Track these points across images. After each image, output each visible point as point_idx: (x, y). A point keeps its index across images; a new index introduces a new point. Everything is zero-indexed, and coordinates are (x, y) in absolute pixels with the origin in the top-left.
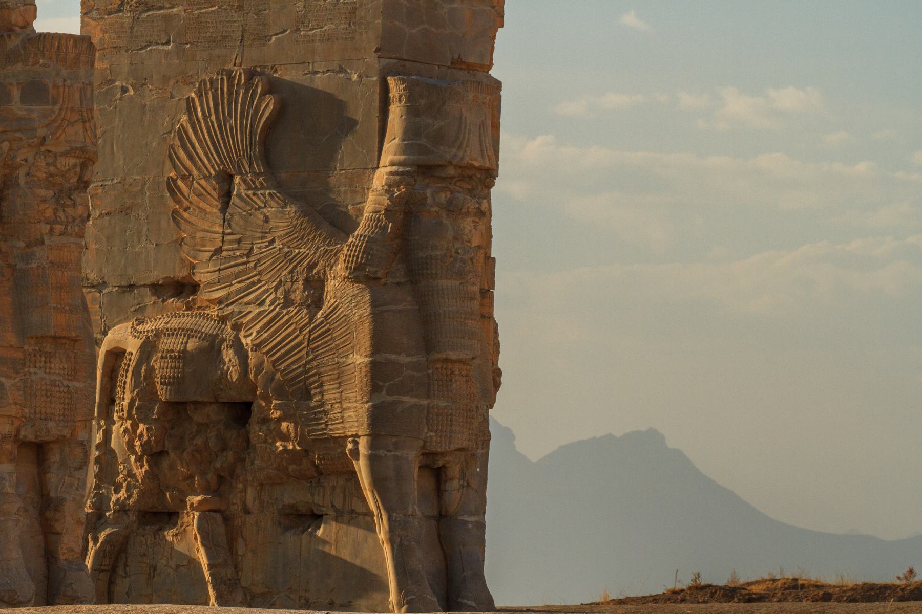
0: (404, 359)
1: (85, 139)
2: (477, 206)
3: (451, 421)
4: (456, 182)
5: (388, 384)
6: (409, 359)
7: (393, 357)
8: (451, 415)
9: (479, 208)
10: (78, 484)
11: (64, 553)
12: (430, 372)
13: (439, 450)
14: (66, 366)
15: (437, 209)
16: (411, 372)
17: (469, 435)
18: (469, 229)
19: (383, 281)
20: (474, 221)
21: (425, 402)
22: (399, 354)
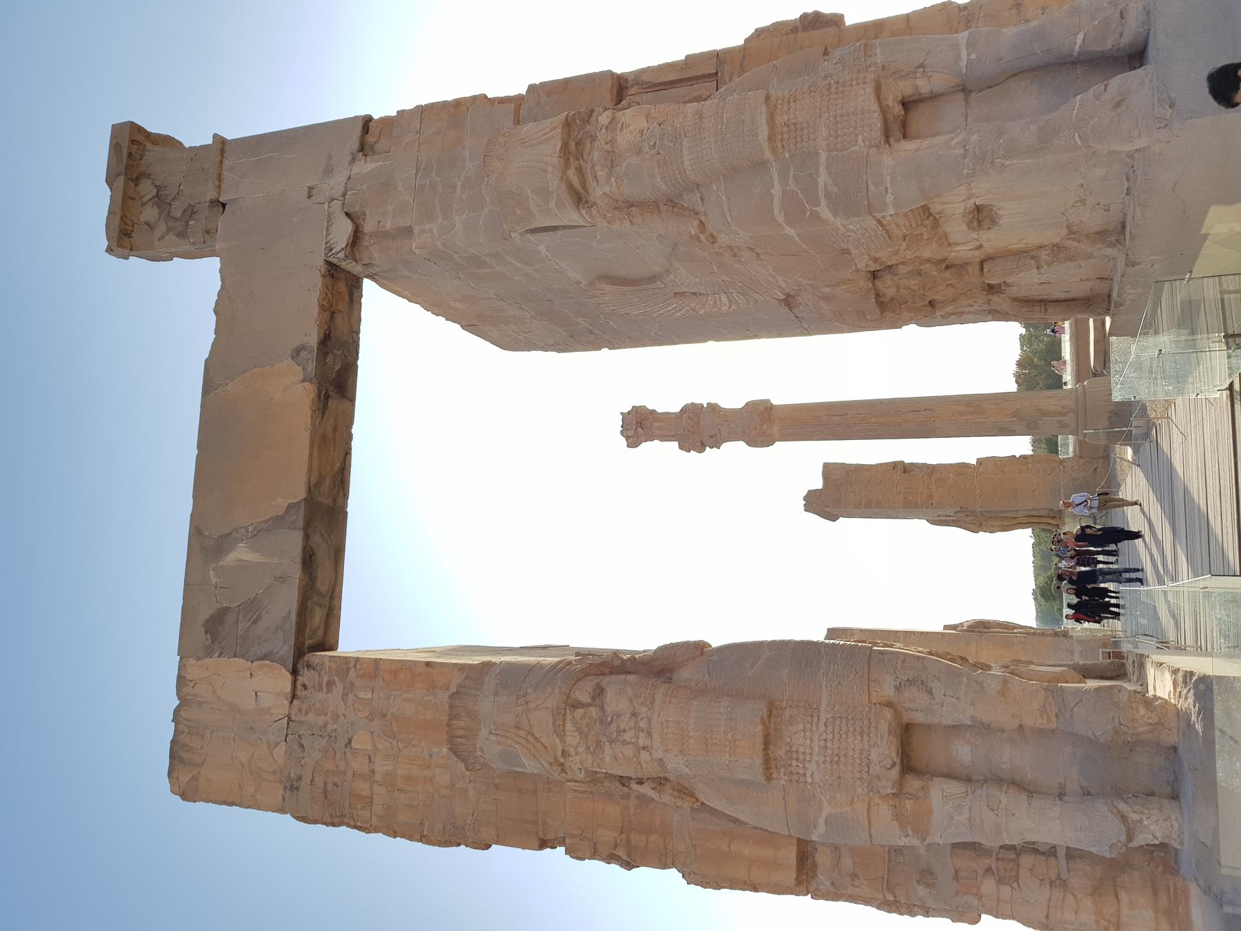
0: (777, 191)
1: (546, 708)
2: (604, 130)
3: (842, 116)
4: (584, 161)
5: (807, 206)
6: (776, 183)
8: (835, 117)
9: (607, 128)
11: (1049, 719)
12: (787, 155)
13: (879, 125)
14: (801, 727)
15: (613, 180)
16: (791, 180)
17: (858, 84)
18: (628, 134)
19: (703, 219)
20: (621, 129)
21: (823, 156)
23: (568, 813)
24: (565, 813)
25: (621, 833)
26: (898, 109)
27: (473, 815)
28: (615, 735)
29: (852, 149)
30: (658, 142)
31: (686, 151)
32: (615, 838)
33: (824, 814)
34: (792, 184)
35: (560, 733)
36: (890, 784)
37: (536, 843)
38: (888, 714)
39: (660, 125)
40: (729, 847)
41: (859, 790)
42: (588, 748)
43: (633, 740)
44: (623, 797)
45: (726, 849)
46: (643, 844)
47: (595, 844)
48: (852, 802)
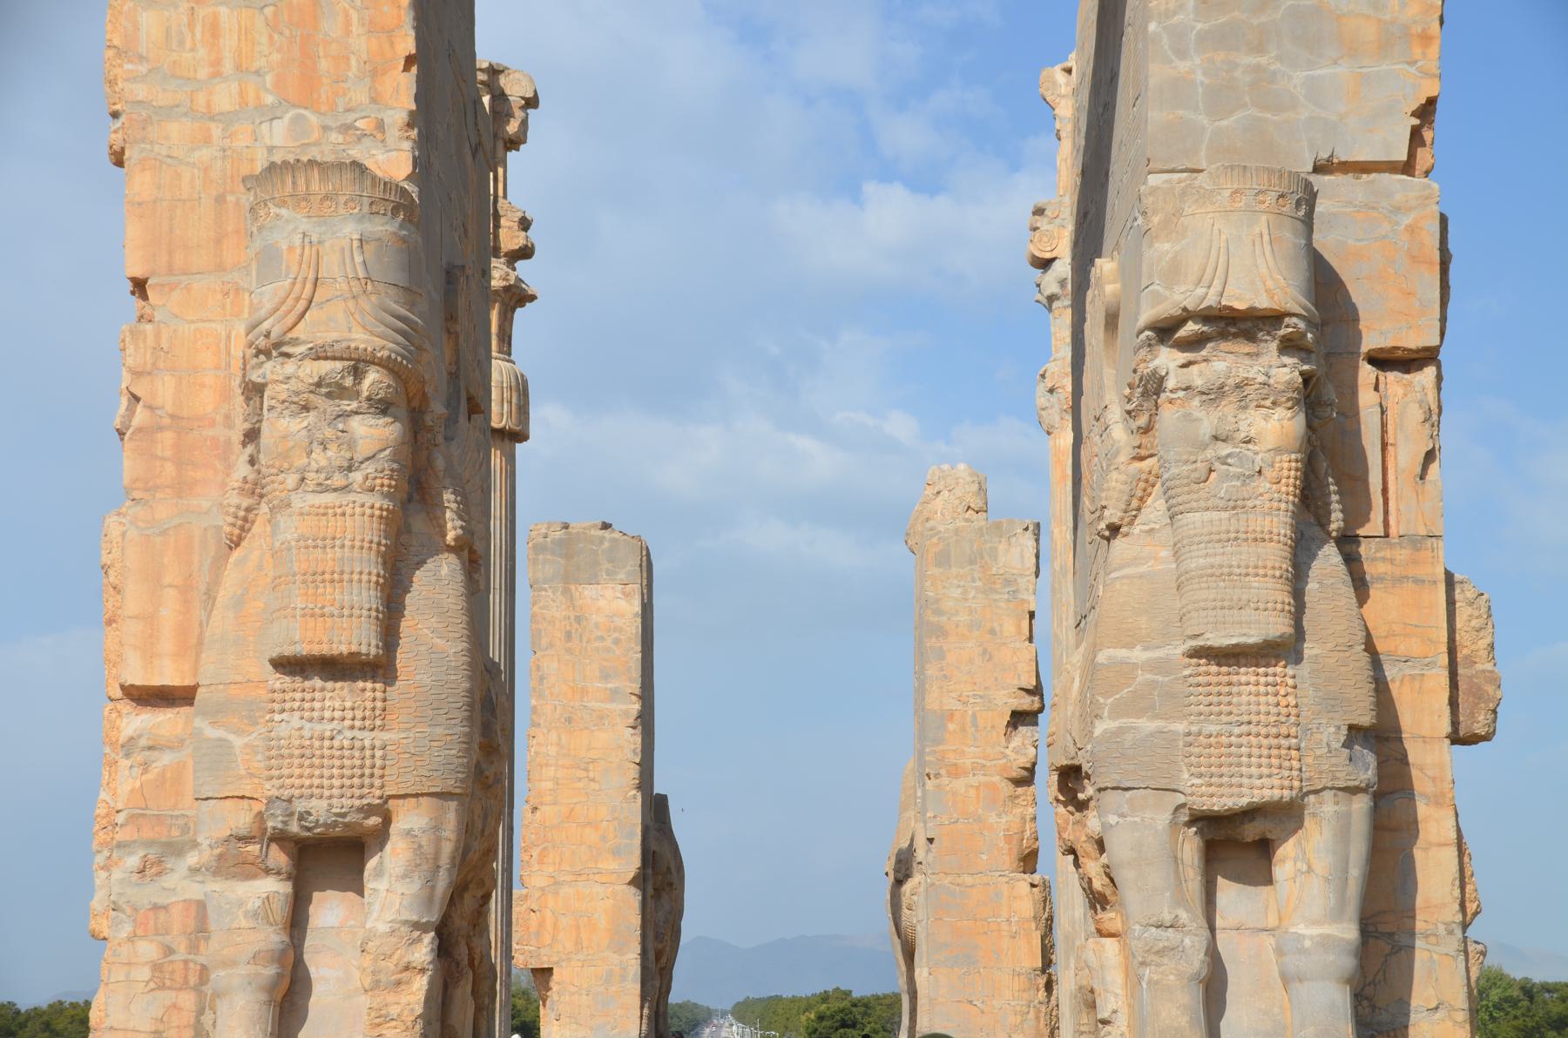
0: (1138, 655)
2: (1261, 378)
7: (1122, 653)
10: (400, 904)
13: (1216, 808)
16: (1149, 676)
21: (1180, 727)
22: (1131, 646)
23: (193, 326)
24: (192, 322)
25: (172, 416)
26: (1251, 832)
27: (169, 157)
28: (319, 436)
29: (1184, 768)
30: (1231, 468)
31: (1208, 515)
32: (163, 407)
33: (231, 737)
34: (1143, 677)
35: (319, 355)
36: (280, 826)
37: (138, 272)
38: (374, 821)
39: (1260, 472)
40: (170, 586)
41: (268, 786)
42: (297, 393)
43: (313, 463)
44: (227, 417)
45: (167, 580)
46: (159, 453)
47: (149, 374)
48: (252, 775)
